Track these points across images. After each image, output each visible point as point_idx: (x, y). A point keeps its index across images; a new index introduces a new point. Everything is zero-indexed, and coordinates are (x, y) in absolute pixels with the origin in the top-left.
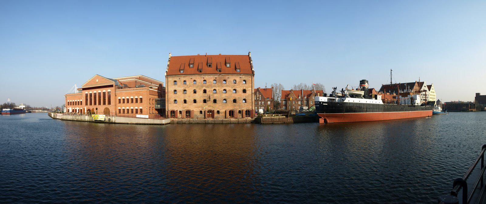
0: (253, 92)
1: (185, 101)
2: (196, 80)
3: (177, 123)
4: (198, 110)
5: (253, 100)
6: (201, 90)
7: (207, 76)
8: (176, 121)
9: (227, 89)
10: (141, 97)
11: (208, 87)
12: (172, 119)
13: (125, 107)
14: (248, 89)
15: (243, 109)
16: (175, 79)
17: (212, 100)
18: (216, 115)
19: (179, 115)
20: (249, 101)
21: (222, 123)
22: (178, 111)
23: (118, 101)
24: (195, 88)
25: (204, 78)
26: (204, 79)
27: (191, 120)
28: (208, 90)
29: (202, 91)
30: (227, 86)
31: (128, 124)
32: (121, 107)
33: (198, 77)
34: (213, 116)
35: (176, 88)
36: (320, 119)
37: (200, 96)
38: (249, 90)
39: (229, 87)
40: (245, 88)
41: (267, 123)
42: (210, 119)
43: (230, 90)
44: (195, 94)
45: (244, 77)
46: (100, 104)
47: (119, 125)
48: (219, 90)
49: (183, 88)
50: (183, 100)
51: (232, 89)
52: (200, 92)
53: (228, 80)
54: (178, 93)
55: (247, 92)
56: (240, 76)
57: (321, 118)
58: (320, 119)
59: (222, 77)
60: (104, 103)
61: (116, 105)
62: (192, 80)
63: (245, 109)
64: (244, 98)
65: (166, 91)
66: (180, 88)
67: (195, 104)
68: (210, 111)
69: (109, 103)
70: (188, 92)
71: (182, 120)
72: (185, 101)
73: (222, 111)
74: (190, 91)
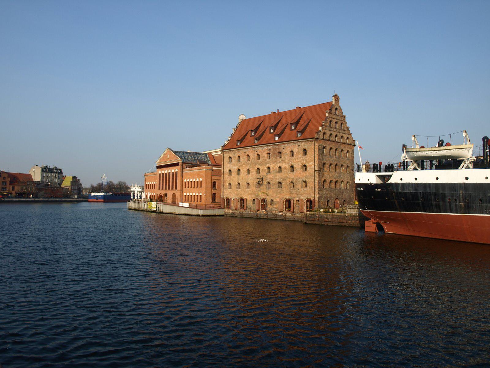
0: (316, 168)
2: (250, 155)
3: (231, 216)
4: (251, 198)
5: (316, 182)
6: (254, 169)
7: (260, 148)
8: (229, 214)
10: (201, 179)
11: (261, 164)
12: (227, 210)
14: (309, 164)
15: (302, 197)
18: (269, 207)
19: (233, 205)
20: (310, 184)
21: (275, 219)
22: (232, 199)
23: (184, 184)
24: (248, 167)
25: (257, 151)
27: (244, 212)
29: (256, 170)
30: (282, 161)
31: (216, 216)
33: (251, 150)
34: (264, 207)
36: (366, 222)
37: (252, 178)
38: (310, 166)
39: (285, 162)
40: (304, 163)
41: (312, 222)
42: (262, 212)
43: (285, 168)
44: (248, 175)
45: (304, 145)
46: (169, 189)
47: (197, 217)
50: (236, 184)
51: (288, 166)
52: (253, 172)
53: (284, 152)
54: (233, 174)
55: (308, 169)
56: (298, 144)
57: (368, 219)
58: (366, 222)
59: (277, 147)
60: (172, 188)
61: (182, 190)
62: (246, 156)
63: (304, 198)
64: (304, 179)
65: (222, 171)
66: (234, 168)
68: (264, 200)
69: (176, 188)
70: (241, 173)
71: (235, 213)
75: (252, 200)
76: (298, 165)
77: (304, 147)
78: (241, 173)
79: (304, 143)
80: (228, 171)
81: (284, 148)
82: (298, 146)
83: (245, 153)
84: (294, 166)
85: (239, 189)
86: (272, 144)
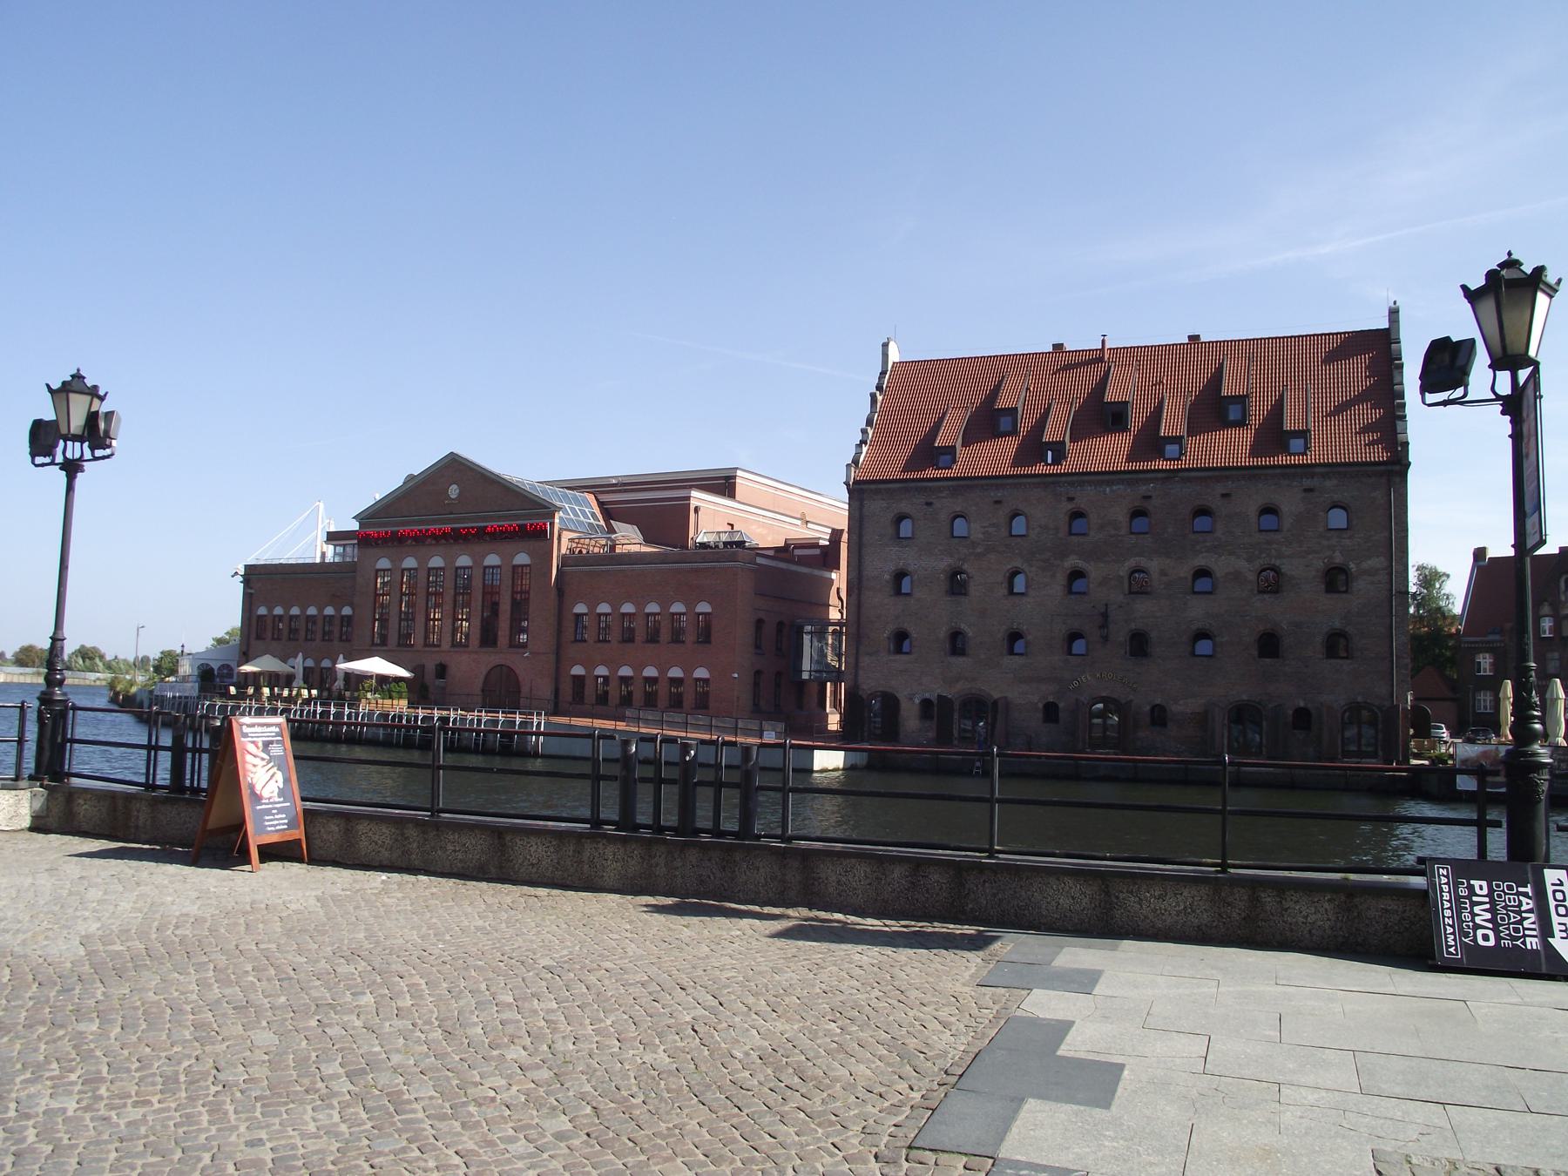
1: (957, 643)
9: (1221, 565)
10: (704, 607)
13: (614, 665)
14: (1366, 565)
16: (904, 507)
17: (1120, 633)
23: (569, 626)
24: (1018, 563)
25: (1071, 499)
26: (1070, 506)
28: (1095, 571)
29: (1061, 579)
32: (590, 665)
35: (909, 559)
40: (1338, 559)
43: (1236, 576)
48: (1163, 573)
49: (944, 563)
50: (943, 633)
51: (1247, 568)
55: (1361, 585)
56: (1307, 483)
64: (1337, 624)
67: (1017, 661)
72: (957, 643)
73: (1184, 706)
74: (984, 578)
75: (1041, 706)
76: (1302, 568)
77: (1336, 497)
78: (974, 590)
79: (1335, 482)
80: (887, 577)
81: (1224, 496)
82: (1309, 490)
83: (997, 502)
84: (1285, 569)
85: (961, 659)
86: (1160, 475)
